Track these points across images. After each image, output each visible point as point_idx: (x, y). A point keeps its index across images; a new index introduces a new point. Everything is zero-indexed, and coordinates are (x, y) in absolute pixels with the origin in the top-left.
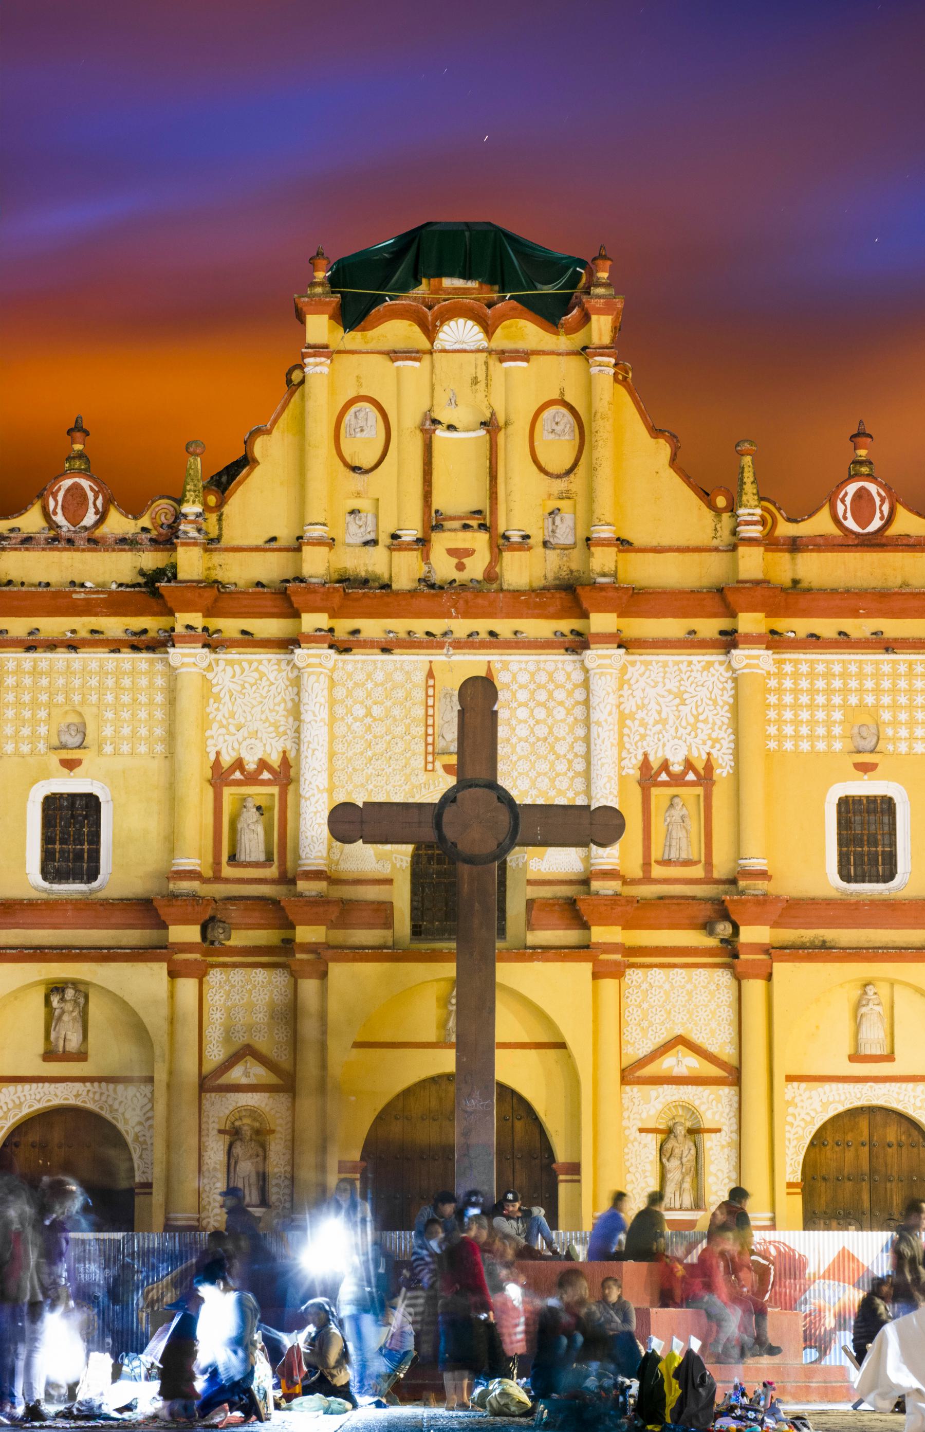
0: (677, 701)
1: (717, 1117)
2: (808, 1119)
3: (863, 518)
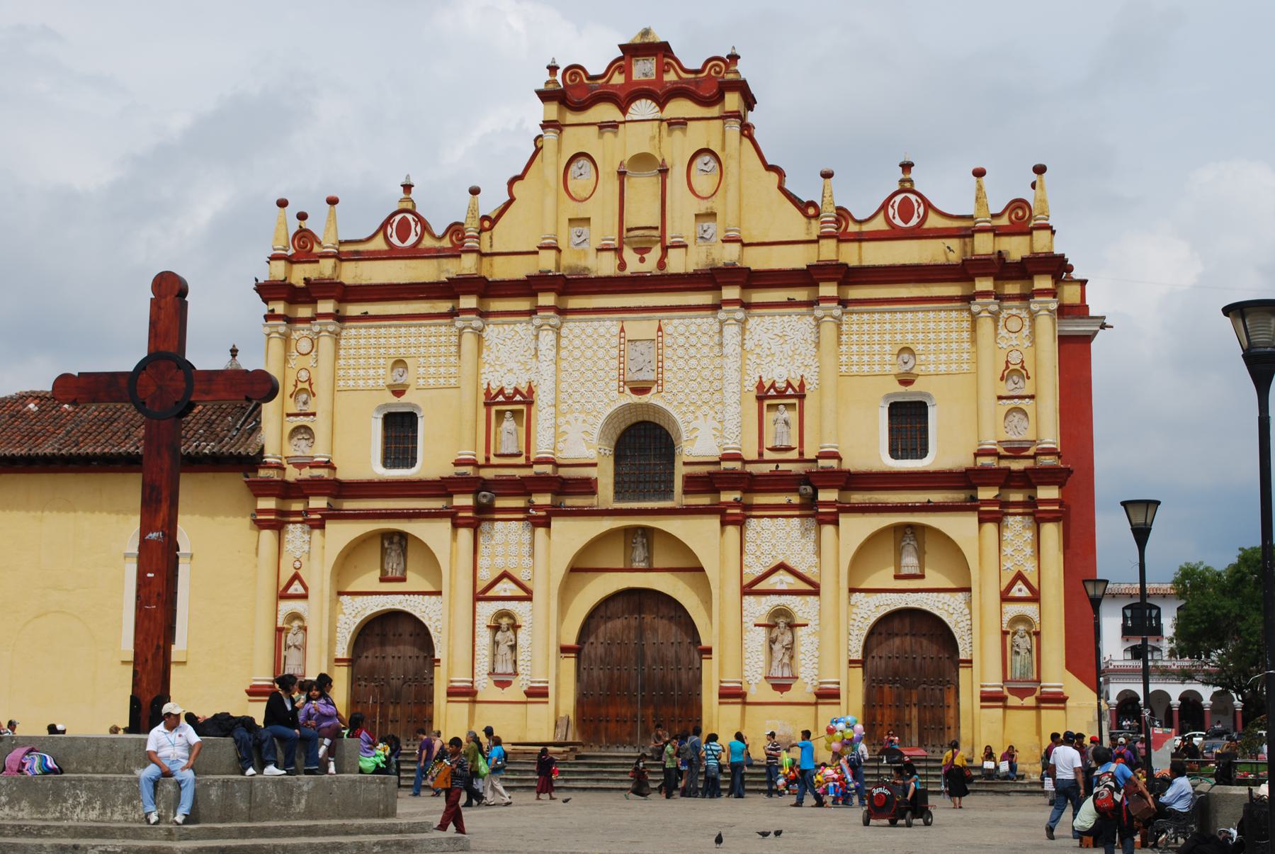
1: (805, 616)
2: (866, 616)
3: (906, 218)
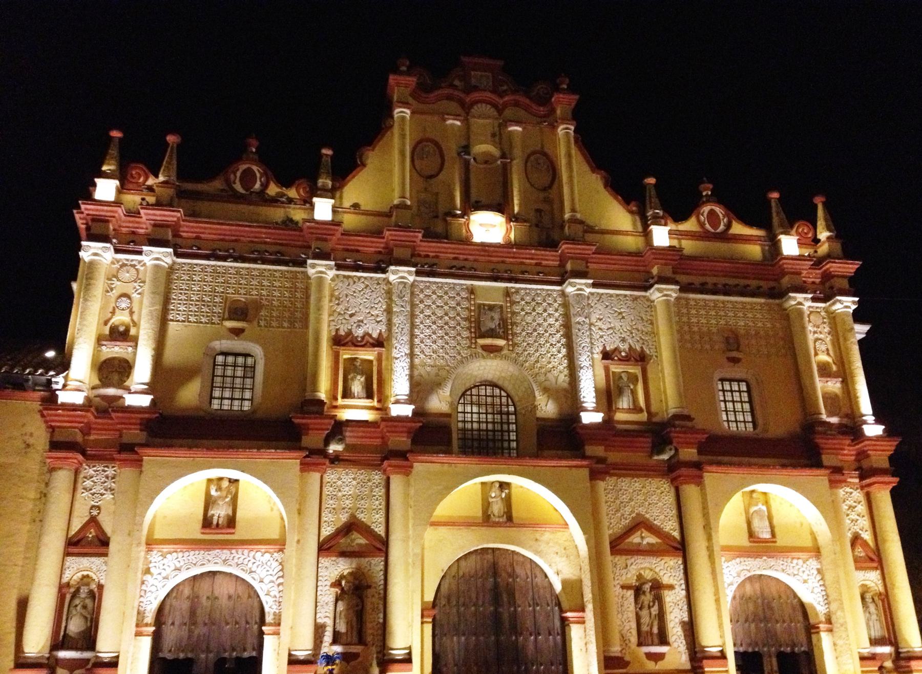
0: (620, 317)
3: (715, 224)
